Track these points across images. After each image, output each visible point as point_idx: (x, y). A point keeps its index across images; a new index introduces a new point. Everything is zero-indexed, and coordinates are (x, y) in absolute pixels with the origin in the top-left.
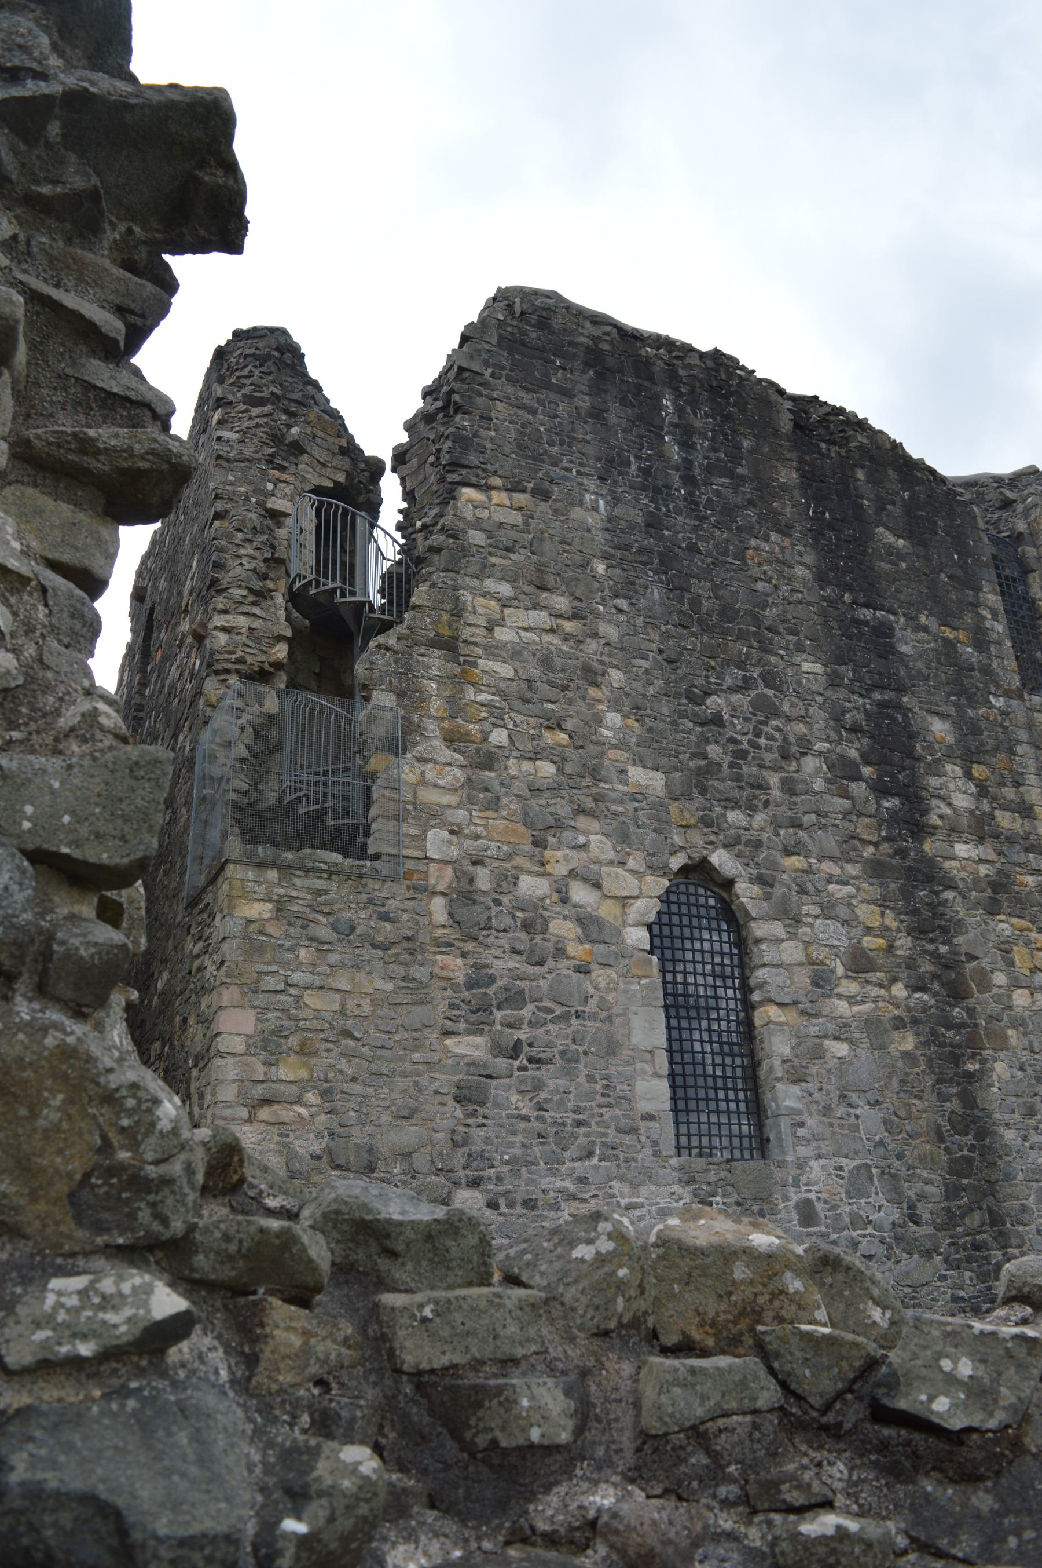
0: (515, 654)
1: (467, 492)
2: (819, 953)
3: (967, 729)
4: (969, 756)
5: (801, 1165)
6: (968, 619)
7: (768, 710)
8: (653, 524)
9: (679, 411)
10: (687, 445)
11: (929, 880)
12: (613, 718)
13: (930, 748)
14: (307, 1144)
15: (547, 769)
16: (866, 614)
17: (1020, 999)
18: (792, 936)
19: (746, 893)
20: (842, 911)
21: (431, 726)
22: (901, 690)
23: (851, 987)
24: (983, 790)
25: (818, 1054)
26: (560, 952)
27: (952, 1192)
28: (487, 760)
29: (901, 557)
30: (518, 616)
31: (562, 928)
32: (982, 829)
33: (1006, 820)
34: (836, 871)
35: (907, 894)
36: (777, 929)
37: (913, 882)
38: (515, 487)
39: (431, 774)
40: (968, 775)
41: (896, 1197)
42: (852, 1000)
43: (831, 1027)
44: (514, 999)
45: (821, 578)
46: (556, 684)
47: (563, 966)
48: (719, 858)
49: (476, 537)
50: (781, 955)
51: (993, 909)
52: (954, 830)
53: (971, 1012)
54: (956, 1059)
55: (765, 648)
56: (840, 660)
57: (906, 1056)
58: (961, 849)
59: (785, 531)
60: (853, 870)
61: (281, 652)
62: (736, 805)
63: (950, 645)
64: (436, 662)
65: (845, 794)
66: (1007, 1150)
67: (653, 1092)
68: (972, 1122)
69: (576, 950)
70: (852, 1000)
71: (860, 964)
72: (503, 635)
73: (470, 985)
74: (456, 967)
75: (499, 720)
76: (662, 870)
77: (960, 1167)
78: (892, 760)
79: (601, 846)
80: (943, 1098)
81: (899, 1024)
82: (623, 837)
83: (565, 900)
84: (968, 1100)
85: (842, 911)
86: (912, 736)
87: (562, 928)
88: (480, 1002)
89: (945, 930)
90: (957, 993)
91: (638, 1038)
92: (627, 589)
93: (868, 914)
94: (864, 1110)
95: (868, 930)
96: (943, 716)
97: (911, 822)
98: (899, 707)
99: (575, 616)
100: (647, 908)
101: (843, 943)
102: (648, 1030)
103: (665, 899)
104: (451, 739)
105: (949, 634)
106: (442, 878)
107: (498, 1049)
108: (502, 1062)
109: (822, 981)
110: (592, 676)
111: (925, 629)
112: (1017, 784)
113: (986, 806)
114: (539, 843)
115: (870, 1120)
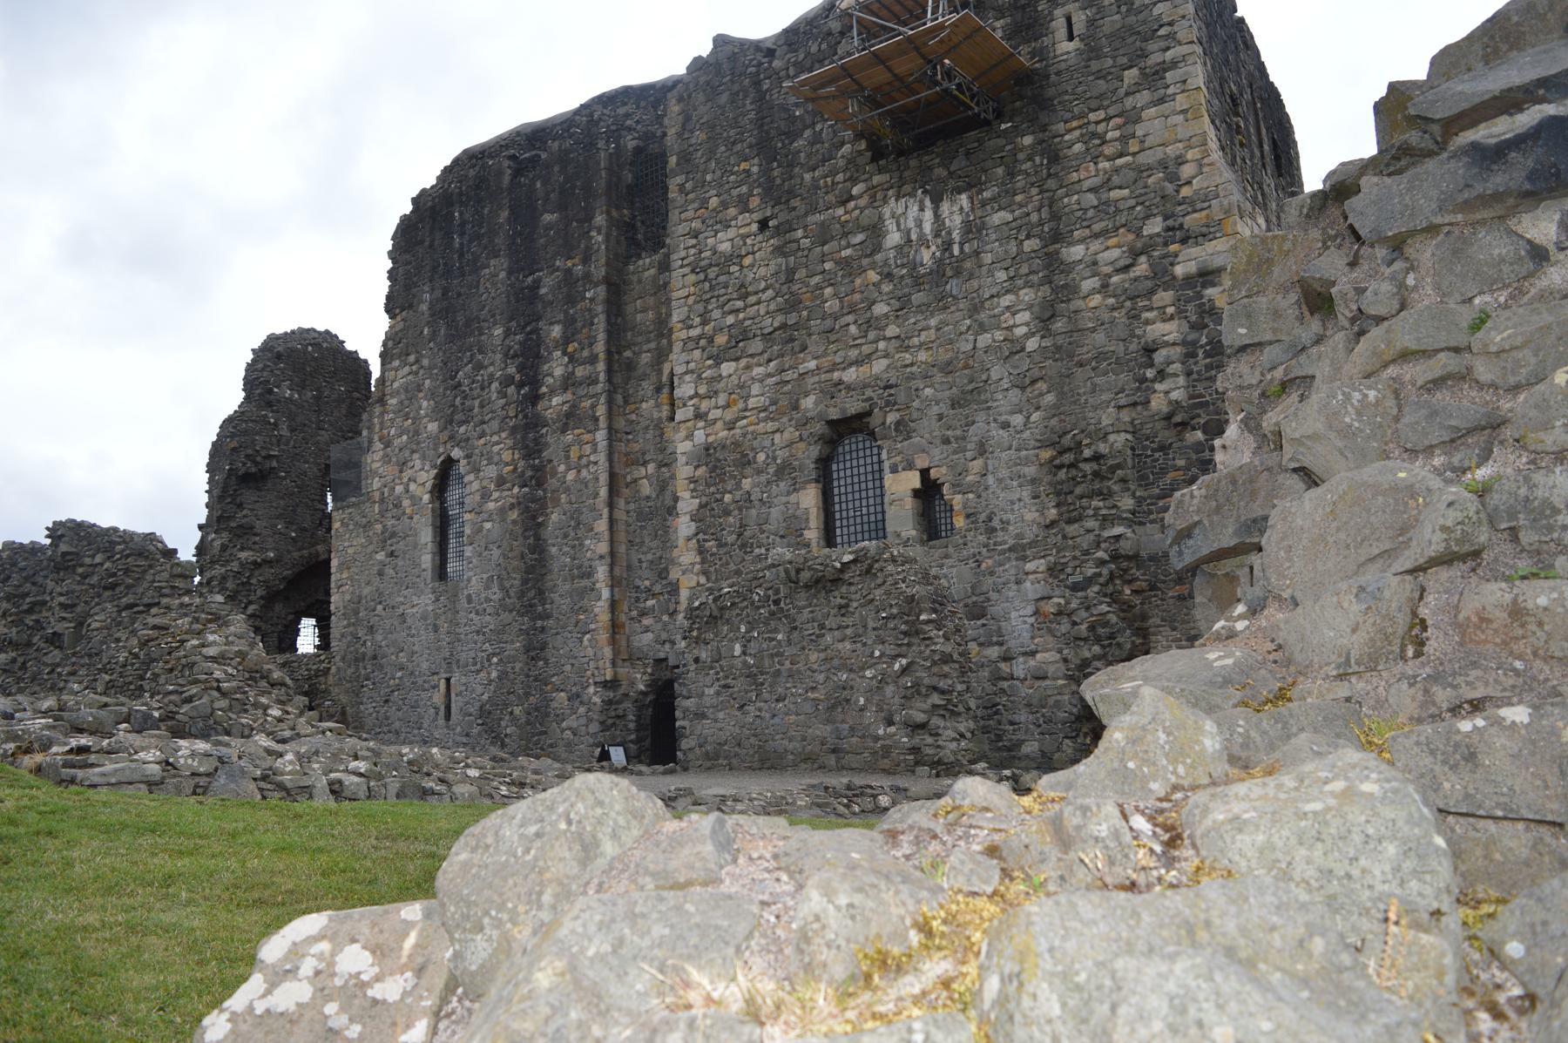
0: (398, 392)
3: (569, 323)
5: (469, 580)
8: (445, 292)
9: (461, 214)
11: (536, 425)
12: (425, 404)
14: (348, 597)
16: (530, 279)
17: (571, 476)
20: (496, 459)
22: (539, 318)
23: (496, 495)
24: (572, 359)
25: (480, 529)
27: (525, 582)
29: (549, 227)
30: (401, 373)
34: (495, 438)
35: (524, 438)
36: (471, 477)
40: (565, 353)
41: (502, 588)
42: (496, 501)
43: (485, 516)
44: (393, 535)
45: (510, 273)
48: (456, 453)
52: (552, 392)
53: (545, 491)
54: (534, 518)
56: (512, 319)
57: (514, 522)
60: (504, 435)
63: (568, 271)
64: (378, 410)
65: (505, 396)
66: (552, 557)
68: (539, 547)
70: (496, 501)
72: (396, 385)
76: (434, 467)
77: (529, 570)
80: (526, 538)
81: (512, 507)
82: (423, 458)
83: (407, 491)
84: (537, 538)
85: (496, 459)
86: (539, 346)
89: (540, 451)
90: (540, 484)
91: (423, 541)
93: (507, 456)
95: (507, 464)
96: (558, 322)
101: (494, 475)
105: (569, 263)
106: (377, 496)
109: (485, 495)
111: (557, 270)
112: (591, 345)
115: (496, 553)
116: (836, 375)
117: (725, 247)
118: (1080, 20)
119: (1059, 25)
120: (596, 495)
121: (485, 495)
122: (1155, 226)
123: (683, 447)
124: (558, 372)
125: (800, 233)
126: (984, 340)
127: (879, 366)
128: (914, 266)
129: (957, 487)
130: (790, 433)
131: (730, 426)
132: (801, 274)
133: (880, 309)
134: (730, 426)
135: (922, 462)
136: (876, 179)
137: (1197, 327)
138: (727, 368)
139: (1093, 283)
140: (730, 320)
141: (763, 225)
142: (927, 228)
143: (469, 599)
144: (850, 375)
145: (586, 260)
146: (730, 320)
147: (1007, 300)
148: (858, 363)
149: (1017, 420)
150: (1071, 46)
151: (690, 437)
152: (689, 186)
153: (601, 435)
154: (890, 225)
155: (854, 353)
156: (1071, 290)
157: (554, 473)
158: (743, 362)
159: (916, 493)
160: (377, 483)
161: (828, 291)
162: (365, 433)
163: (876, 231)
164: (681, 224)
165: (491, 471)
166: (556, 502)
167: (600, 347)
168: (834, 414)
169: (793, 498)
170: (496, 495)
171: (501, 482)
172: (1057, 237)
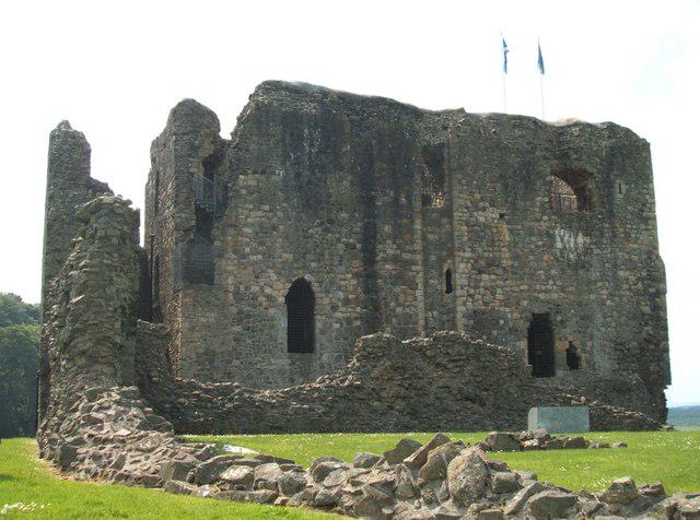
1: (241, 177)
2: (334, 301)
3: (397, 227)
4: (395, 238)
5: (321, 355)
6: (406, 188)
7: (327, 230)
9: (310, 133)
10: (312, 145)
13: (381, 236)
14: (201, 351)
15: (260, 257)
17: (399, 310)
18: (327, 296)
19: (315, 287)
21: (230, 250)
23: (341, 309)
26: (260, 305)
28: (244, 256)
31: (262, 299)
32: (395, 259)
33: (406, 256)
35: (365, 282)
37: (368, 277)
38: (254, 173)
39: (228, 266)
44: (248, 316)
46: (264, 231)
47: (262, 309)
49: (244, 192)
50: (323, 301)
51: (394, 284)
52: (385, 260)
55: (330, 211)
58: (388, 266)
59: (342, 169)
61: (193, 223)
62: (314, 261)
67: (282, 336)
69: (264, 304)
71: (346, 302)
72: (249, 220)
73: (238, 313)
74: (234, 310)
75: (247, 244)
78: (370, 238)
79: (274, 277)
81: (356, 319)
87: (262, 299)
88: (241, 317)
90: (376, 309)
92: (287, 199)
94: (342, 340)
97: (370, 258)
98: (375, 225)
99: (271, 211)
100: (286, 292)
102: (283, 323)
103: (290, 289)
104: (235, 252)
106: (231, 288)
107: (244, 329)
108: (245, 332)
110: (274, 228)
113: (399, 252)
114: (257, 277)
116: (536, 294)
117: (482, 219)
118: (623, 186)
119: (617, 185)
120: (417, 323)
121: (334, 308)
122: (644, 274)
123: (461, 309)
124: (390, 252)
125: (519, 227)
126: (592, 297)
127: (555, 296)
128: (569, 260)
129: (584, 351)
130: (516, 315)
131: (486, 304)
132: (520, 245)
133: (553, 272)
134: (486, 304)
135: (570, 338)
136: (553, 217)
137: (653, 310)
138: (485, 277)
139: (625, 286)
140: (486, 254)
141: (502, 216)
142: (572, 245)
143: (322, 367)
144: (542, 296)
145: (408, 197)
146: (486, 254)
147: (600, 284)
148: (545, 291)
149: (604, 329)
150: (621, 196)
151: (464, 304)
152: (464, 181)
153: (419, 293)
154: (558, 239)
155: (544, 288)
156: (618, 287)
157: (387, 305)
158: (493, 277)
159: (567, 350)
160: (230, 281)
161: (532, 257)
162: (217, 243)
163: (551, 237)
164: (461, 199)
165: (341, 295)
166: (389, 322)
167: (418, 246)
168: (536, 311)
169: (518, 343)
170: (341, 309)
171: (346, 302)
172: (615, 266)
